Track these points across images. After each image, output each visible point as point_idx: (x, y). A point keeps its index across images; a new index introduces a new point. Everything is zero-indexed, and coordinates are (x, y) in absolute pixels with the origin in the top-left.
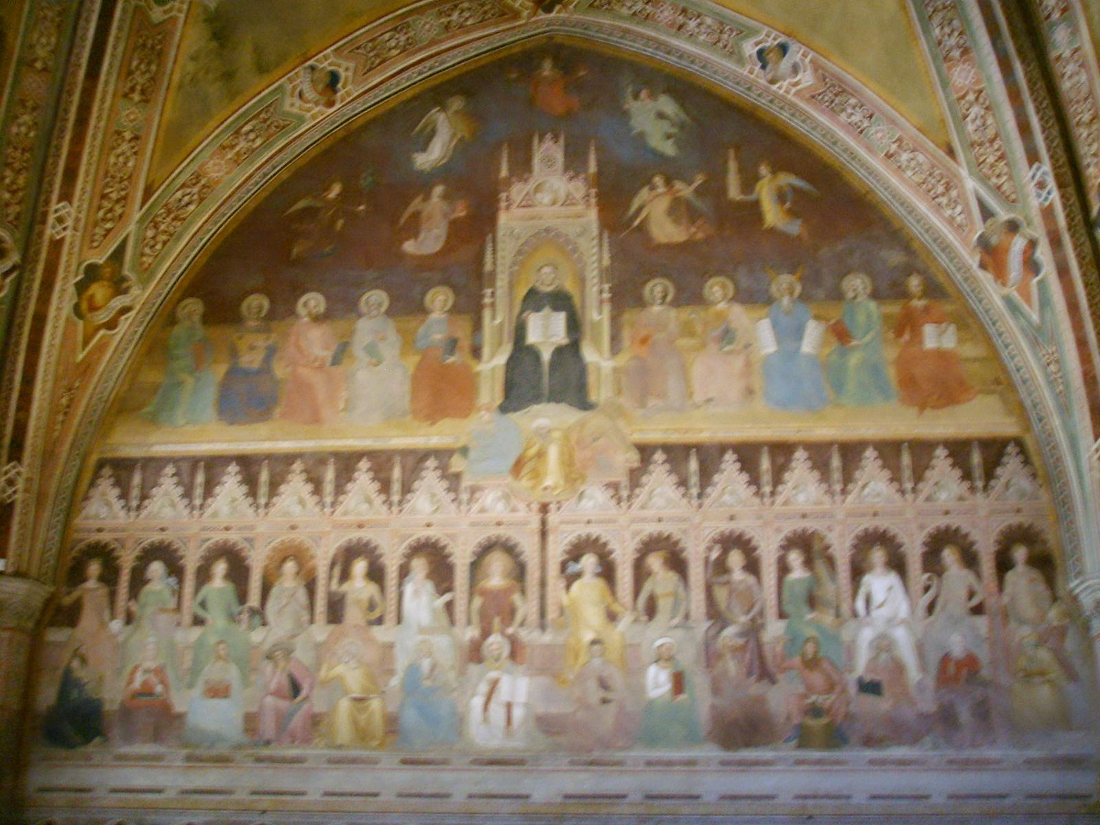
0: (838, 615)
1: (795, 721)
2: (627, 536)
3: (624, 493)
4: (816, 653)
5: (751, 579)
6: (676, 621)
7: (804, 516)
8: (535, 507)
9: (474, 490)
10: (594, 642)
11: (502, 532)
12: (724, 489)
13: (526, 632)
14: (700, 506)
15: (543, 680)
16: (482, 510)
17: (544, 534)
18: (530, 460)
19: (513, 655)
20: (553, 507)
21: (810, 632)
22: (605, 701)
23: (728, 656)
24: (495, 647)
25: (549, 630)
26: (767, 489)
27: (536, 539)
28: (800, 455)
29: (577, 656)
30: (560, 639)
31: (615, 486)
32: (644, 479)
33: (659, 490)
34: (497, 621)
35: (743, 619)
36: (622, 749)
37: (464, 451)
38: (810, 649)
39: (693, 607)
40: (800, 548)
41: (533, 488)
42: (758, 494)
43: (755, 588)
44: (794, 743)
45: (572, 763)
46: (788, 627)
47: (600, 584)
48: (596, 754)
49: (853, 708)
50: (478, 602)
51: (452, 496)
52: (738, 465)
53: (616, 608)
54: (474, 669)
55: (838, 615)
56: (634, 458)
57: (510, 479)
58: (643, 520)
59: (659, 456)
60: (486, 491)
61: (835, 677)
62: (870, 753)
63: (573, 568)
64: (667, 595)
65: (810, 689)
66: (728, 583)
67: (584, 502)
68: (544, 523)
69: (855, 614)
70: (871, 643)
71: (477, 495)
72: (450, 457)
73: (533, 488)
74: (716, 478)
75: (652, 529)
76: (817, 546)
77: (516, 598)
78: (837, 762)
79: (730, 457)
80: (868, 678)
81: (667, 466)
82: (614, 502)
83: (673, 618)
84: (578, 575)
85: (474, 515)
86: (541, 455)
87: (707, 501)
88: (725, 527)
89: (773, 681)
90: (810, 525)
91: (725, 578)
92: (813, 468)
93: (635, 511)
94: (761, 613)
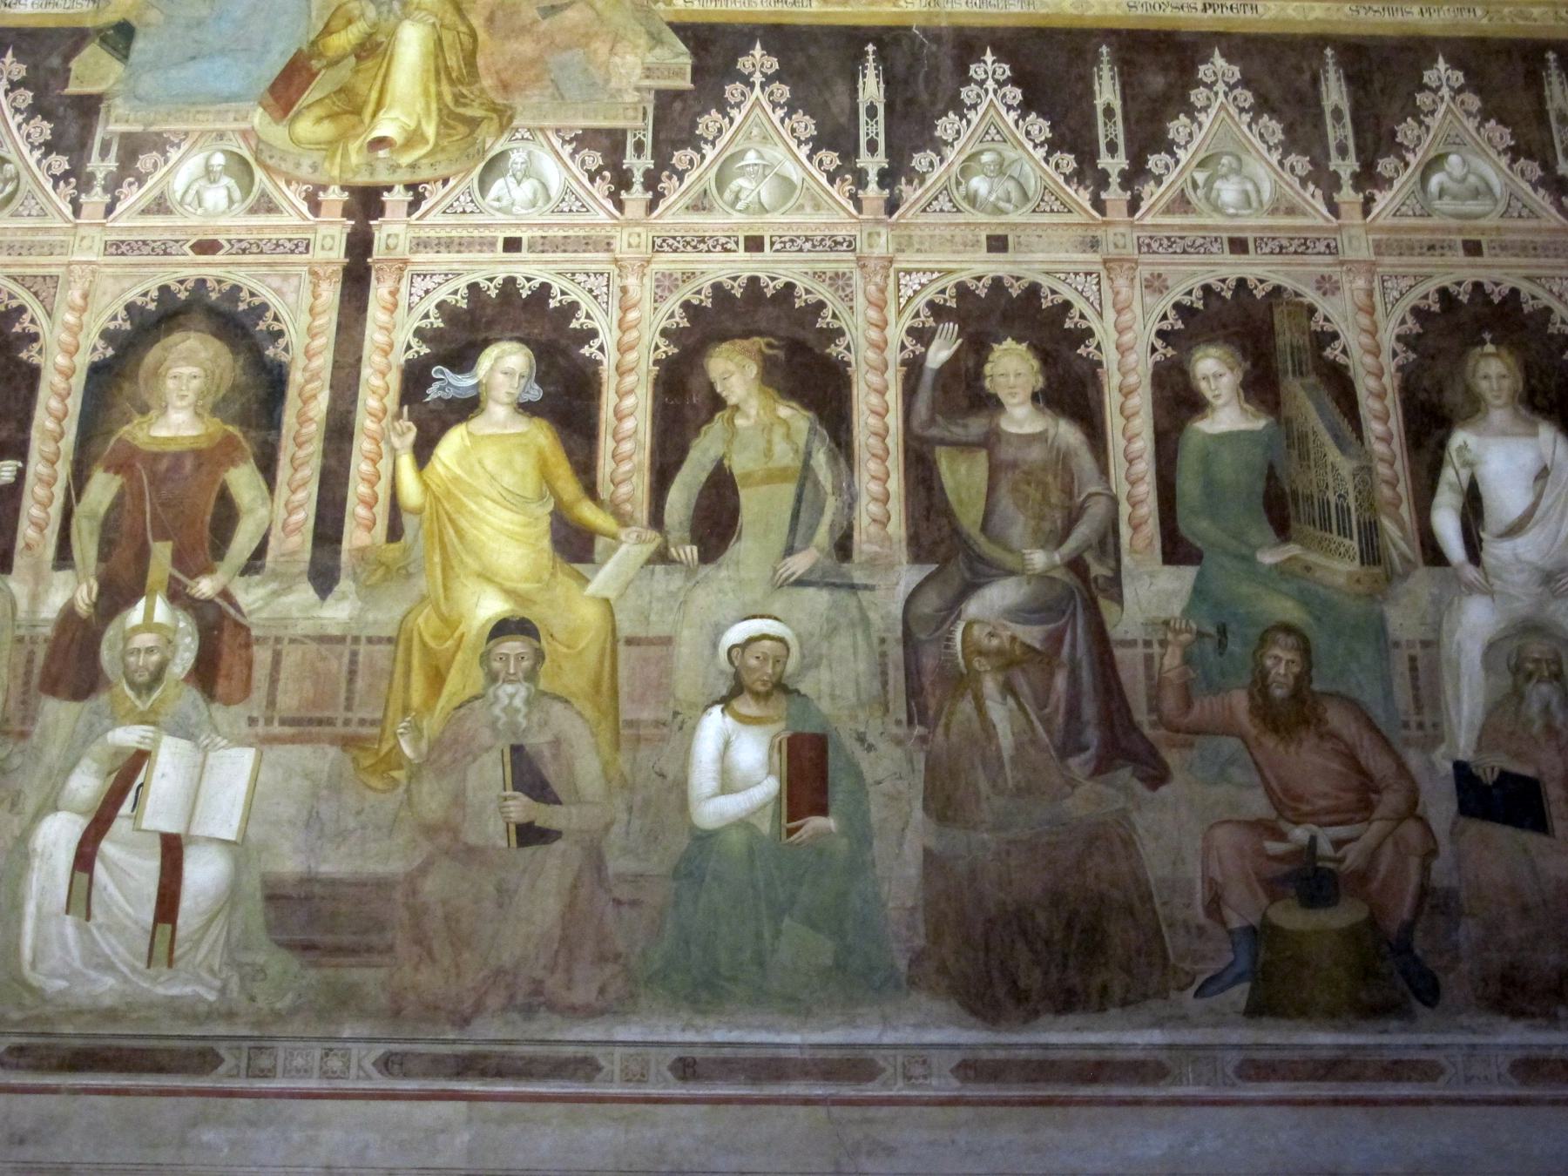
0: (1372, 553)
1: (1242, 911)
2: (640, 288)
3: (638, 164)
4: (1303, 679)
5: (1068, 434)
6: (800, 564)
7: (1238, 246)
8: (335, 197)
9: (132, 148)
10: (502, 629)
11: (212, 269)
12: (971, 157)
13: (261, 592)
14: (892, 206)
15: (320, 759)
16: (160, 206)
17: (356, 279)
18: (334, 63)
19: (206, 673)
20: (396, 199)
21: (1286, 609)
22: (529, 834)
23: (990, 685)
24: (145, 640)
25: (345, 585)
26: (1113, 164)
27: (330, 293)
28: (1217, 68)
29: (437, 679)
30: (385, 616)
31: (612, 143)
32: (709, 122)
33: (751, 157)
34: (162, 554)
35: (1038, 559)
36: (589, 1013)
37: (121, 37)
38: (1281, 662)
39: (866, 510)
40: (1227, 340)
41: (332, 146)
42: (1088, 173)
43: (1085, 460)
44: (1239, 994)
45: (387, 1064)
46: (1199, 592)
47: (541, 434)
48: (490, 1031)
49: (1442, 873)
50: (102, 489)
51: (60, 163)
52: (1015, 94)
53: (589, 513)
54: (58, 714)
55: (1372, 553)
56: (677, 62)
57: (258, 118)
58: (700, 242)
59: (758, 61)
60: (174, 155)
61: (1380, 765)
62: (1516, 1035)
63: (448, 383)
64: (771, 477)
65: (1288, 804)
66: (991, 441)
67: (497, 187)
68: (360, 245)
69: (1433, 553)
70: (1491, 647)
71: (145, 162)
72: (76, 49)
73: (332, 146)
74: (946, 126)
75: (734, 267)
76: (1287, 336)
77: (243, 480)
78: (1395, 1070)
79: (989, 67)
80: (1490, 766)
81: (783, 91)
82: (602, 188)
83: (790, 551)
84: (467, 407)
85: (127, 219)
86: (373, 50)
87: (910, 193)
88: (979, 267)
89: (1157, 776)
90: (1260, 270)
91: (976, 426)
92: (1263, 105)
93: (673, 214)
94: (1108, 543)
